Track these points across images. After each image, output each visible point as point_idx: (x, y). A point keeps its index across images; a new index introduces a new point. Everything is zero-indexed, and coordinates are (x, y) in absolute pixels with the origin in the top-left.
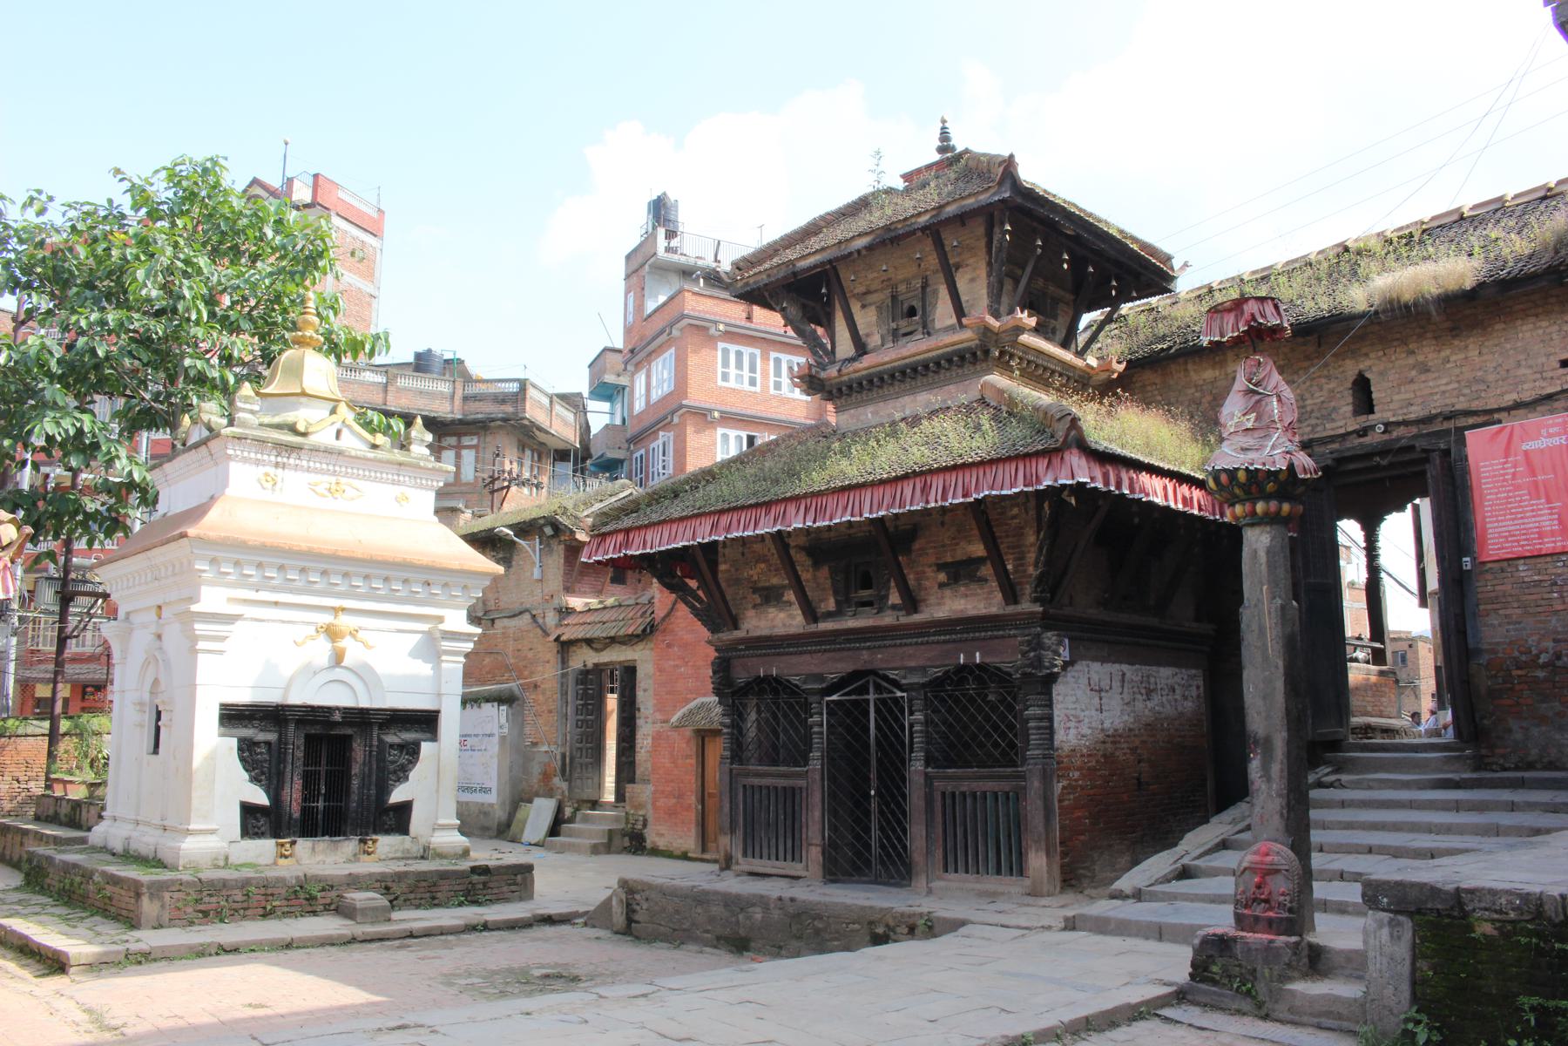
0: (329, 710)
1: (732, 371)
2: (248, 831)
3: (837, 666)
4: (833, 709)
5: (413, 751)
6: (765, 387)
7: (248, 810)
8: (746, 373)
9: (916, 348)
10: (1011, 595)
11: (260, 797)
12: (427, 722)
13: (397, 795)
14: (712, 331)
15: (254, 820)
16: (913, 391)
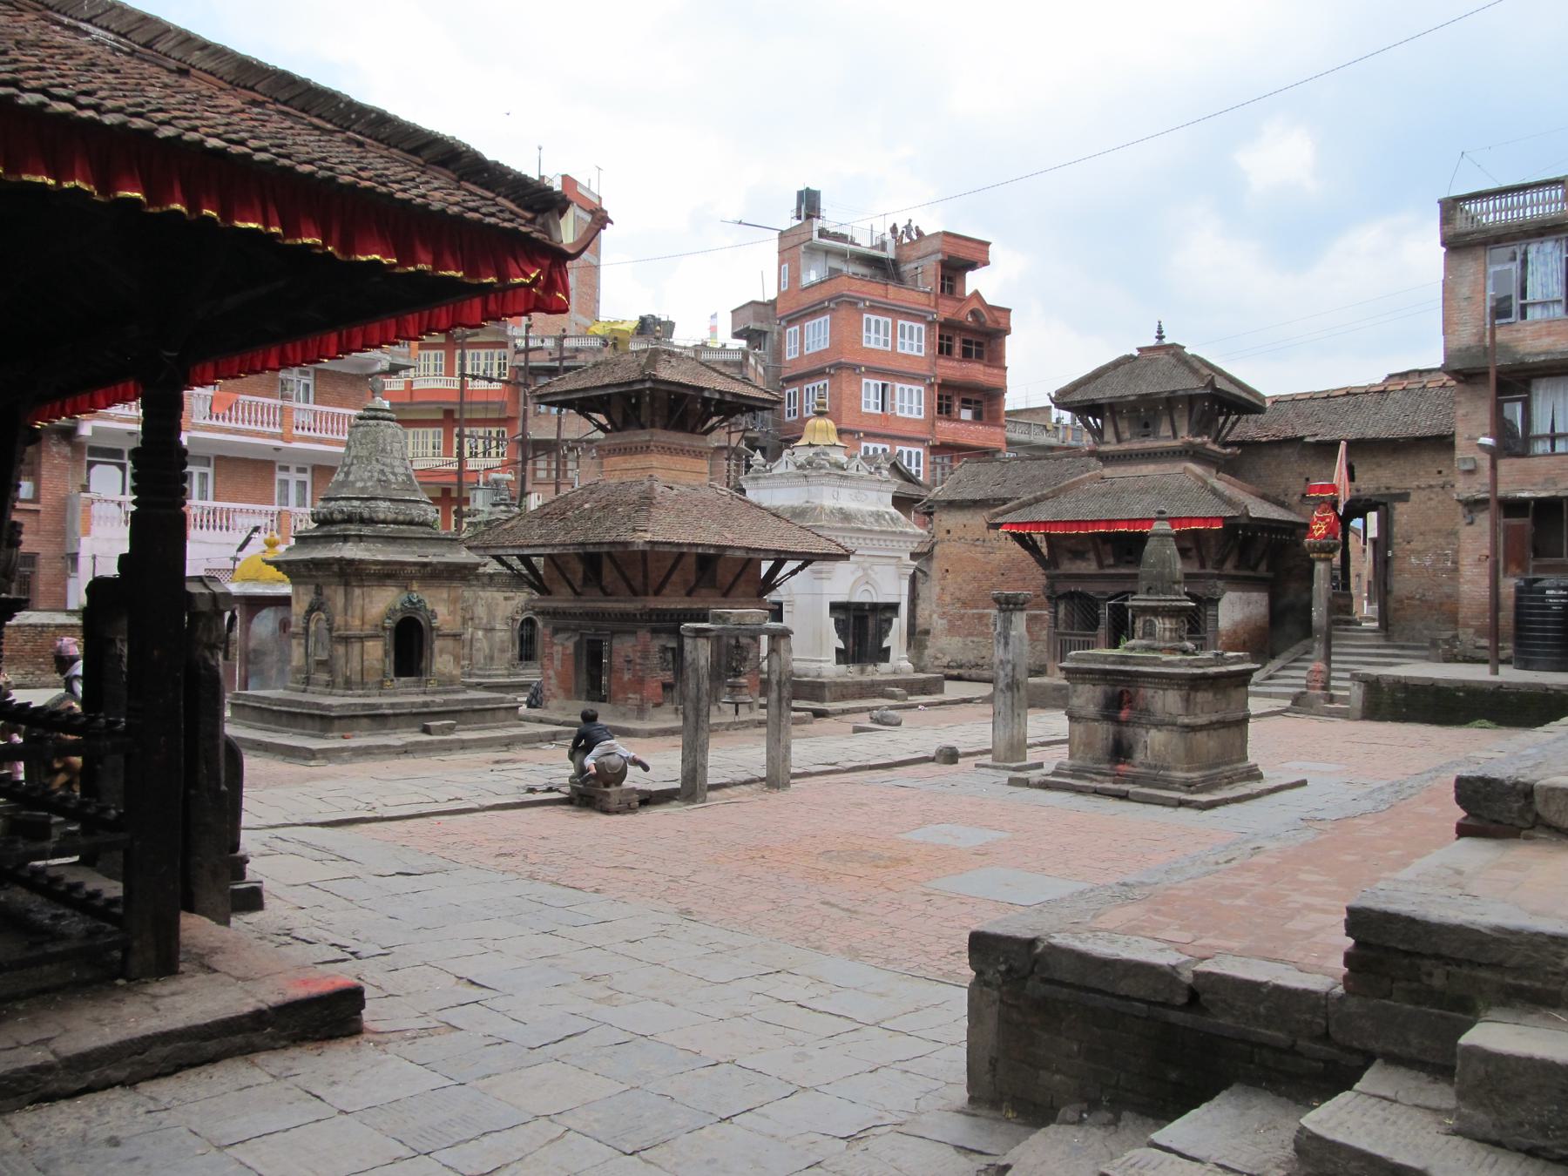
0: (863, 604)
1: (873, 335)
2: (838, 662)
3: (1112, 589)
4: (1111, 607)
5: (890, 622)
6: (894, 347)
7: (838, 651)
8: (882, 337)
9: (1150, 444)
10: (1203, 566)
11: (842, 646)
12: (893, 608)
13: (885, 645)
14: (861, 305)
15: (842, 656)
16: (1147, 463)
